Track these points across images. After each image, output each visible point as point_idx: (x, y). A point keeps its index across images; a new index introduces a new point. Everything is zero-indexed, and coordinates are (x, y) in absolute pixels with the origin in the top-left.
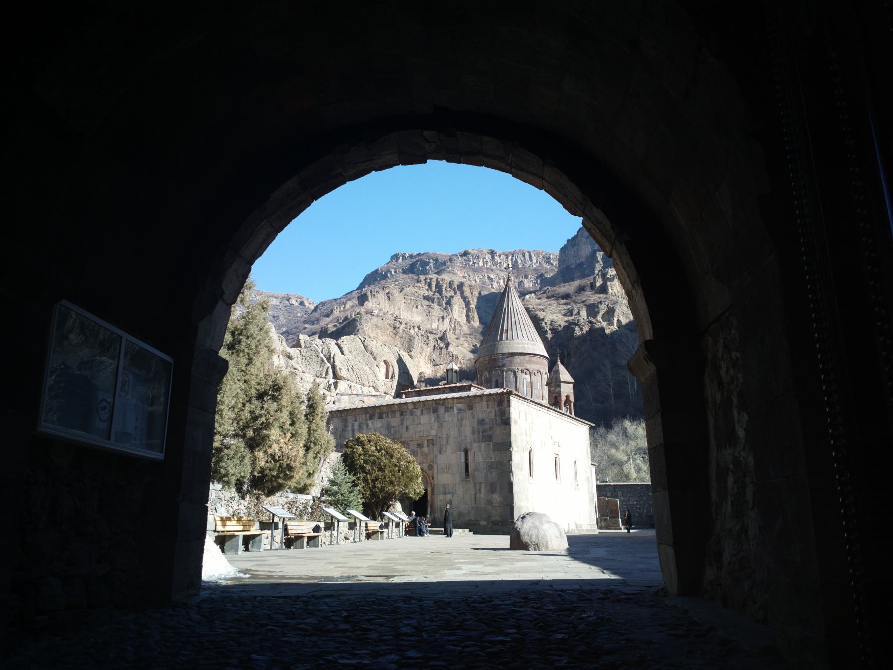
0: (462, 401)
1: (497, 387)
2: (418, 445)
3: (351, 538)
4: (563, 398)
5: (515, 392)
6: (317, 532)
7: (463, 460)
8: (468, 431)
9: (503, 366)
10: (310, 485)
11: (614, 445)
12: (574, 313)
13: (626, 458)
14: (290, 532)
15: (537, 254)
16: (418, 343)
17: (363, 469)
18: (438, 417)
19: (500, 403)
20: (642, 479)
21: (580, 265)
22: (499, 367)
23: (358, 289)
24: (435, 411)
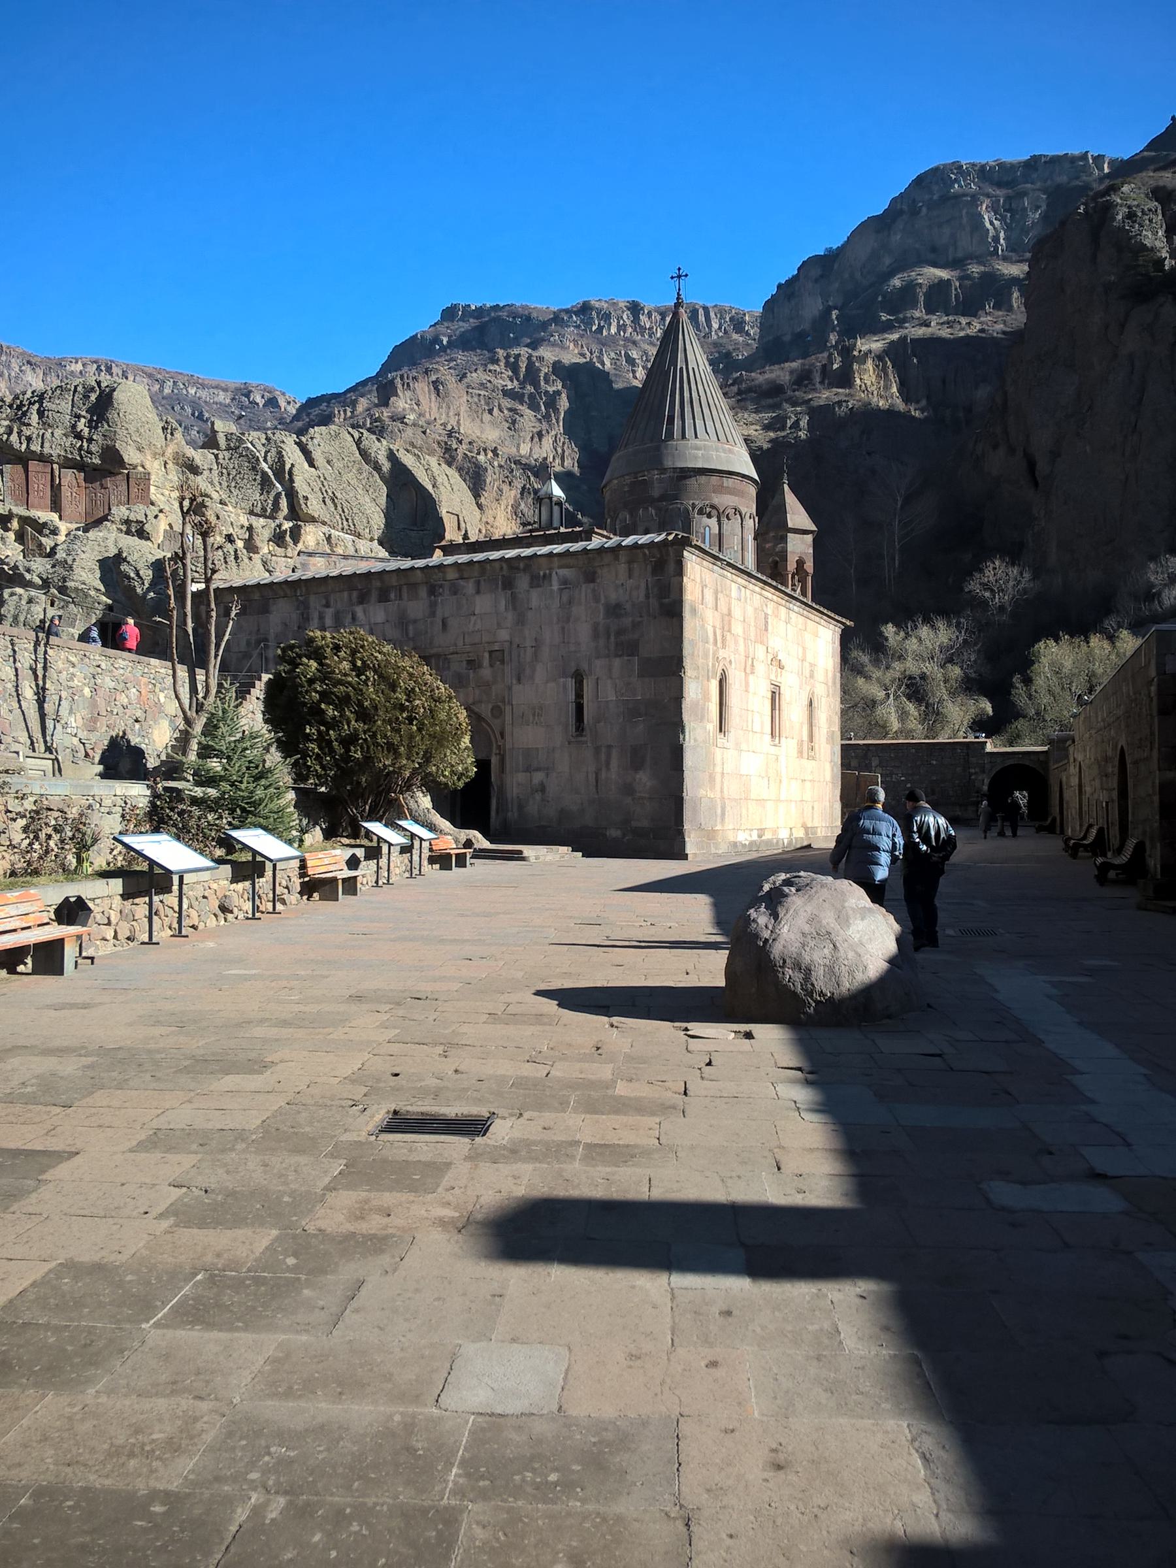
2: (469, 662)
3: (248, 906)
4: (791, 566)
6: (70, 922)
8: (583, 631)
15: (721, 312)
16: (492, 478)
17: (316, 714)
18: (514, 597)
19: (659, 567)
20: (909, 733)
21: (800, 337)
24: (508, 584)
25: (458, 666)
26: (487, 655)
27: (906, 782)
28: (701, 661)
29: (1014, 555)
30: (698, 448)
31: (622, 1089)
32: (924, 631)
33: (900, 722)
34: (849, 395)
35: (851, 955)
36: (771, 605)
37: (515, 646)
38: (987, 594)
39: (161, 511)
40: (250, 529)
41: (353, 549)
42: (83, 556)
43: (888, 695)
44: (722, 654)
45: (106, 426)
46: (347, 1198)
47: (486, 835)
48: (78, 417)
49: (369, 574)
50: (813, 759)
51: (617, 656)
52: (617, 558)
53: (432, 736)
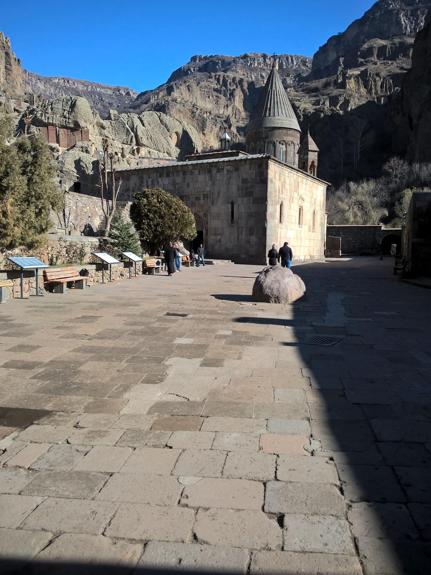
0: (230, 163)
1: (260, 153)
2: (197, 198)
3: (128, 275)
4: (310, 164)
5: (272, 157)
7: (230, 210)
8: (234, 188)
9: (266, 138)
10: (37, 242)
11: (340, 199)
12: (321, 103)
14: (49, 278)
15: (297, 58)
16: (209, 123)
18: (211, 175)
20: (357, 223)
21: (328, 68)
22: (263, 138)
23: (167, 83)
24: (209, 171)
26: (202, 196)
27: (352, 240)
28: (274, 199)
29: (402, 155)
30: (279, 120)
31: (219, 311)
32: (365, 185)
33: (353, 218)
34: (344, 92)
35: (284, 286)
37: (211, 193)
38: (391, 170)
39: (93, 143)
40: (123, 149)
41: (157, 156)
42: (68, 159)
43: (350, 208)
45: (74, 113)
48: (65, 110)
49: (163, 167)
50: (314, 232)
52: (246, 163)
53: (183, 224)
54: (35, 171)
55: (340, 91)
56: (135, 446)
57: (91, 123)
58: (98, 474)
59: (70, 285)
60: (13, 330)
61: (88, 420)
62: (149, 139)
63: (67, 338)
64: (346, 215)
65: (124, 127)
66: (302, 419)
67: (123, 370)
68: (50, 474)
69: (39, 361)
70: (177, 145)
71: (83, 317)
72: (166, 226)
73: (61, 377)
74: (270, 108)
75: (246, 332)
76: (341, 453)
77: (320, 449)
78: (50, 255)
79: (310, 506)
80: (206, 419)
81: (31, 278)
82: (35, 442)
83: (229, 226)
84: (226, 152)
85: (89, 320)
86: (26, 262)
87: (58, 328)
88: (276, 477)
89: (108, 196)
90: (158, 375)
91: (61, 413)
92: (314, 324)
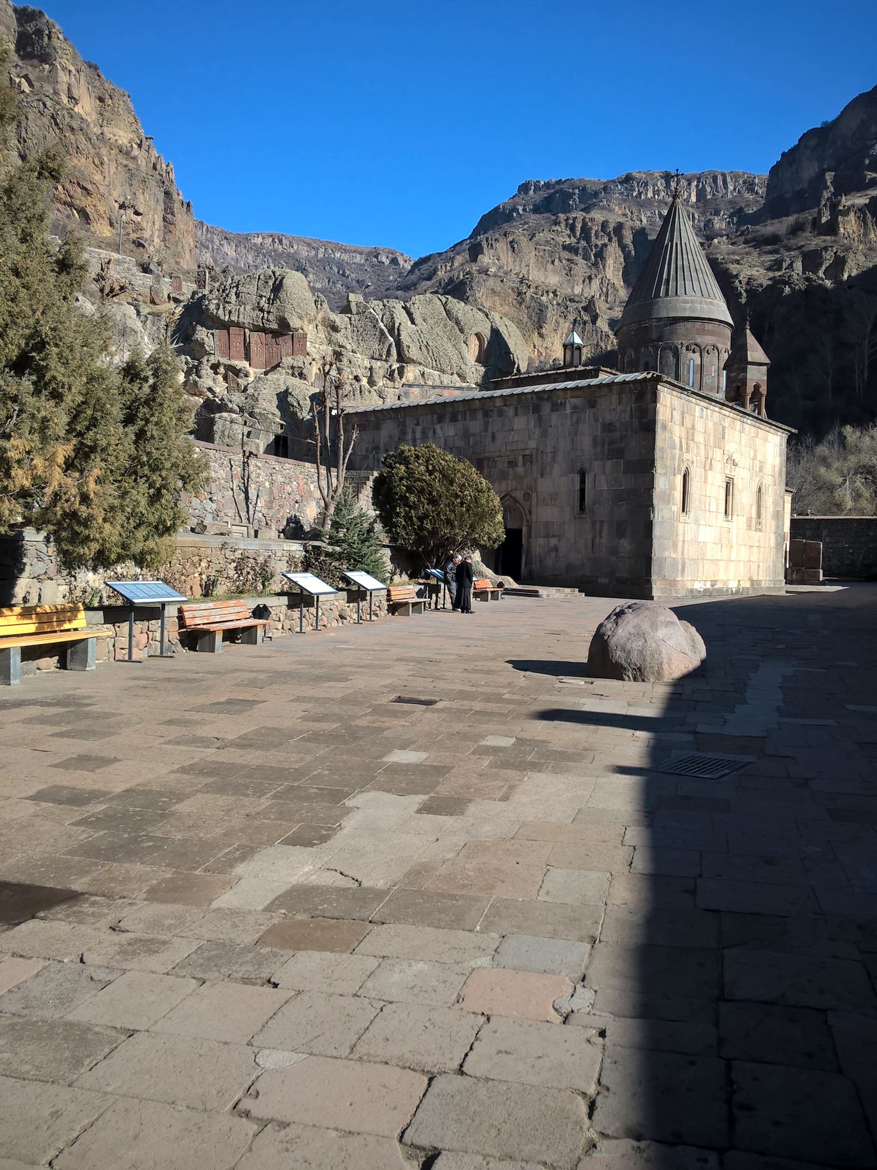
0: (579, 393)
1: (646, 369)
2: (509, 463)
3: (355, 616)
4: (750, 389)
7: (577, 487)
8: (586, 442)
9: (660, 339)
11: (824, 461)
12: (785, 265)
13: (841, 480)
14: (188, 622)
15: (736, 177)
16: (552, 314)
17: (404, 499)
18: (540, 417)
20: (862, 511)
23: (471, 237)
24: (537, 409)
25: (502, 465)
26: (521, 458)
27: (849, 548)
28: (668, 463)
30: (686, 302)
33: (854, 502)
34: (835, 241)
35: (654, 645)
36: (727, 423)
37: (540, 452)
39: (313, 360)
40: (371, 369)
42: (264, 391)
43: (845, 480)
44: (686, 456)
46: (369, 718)
47: (517, 580)
48: (261, 296)
50: (760, 530)
51: (608, 459)
52: (611, 391)
53: (476, 515)
54: (152, 415)
55: (825, 241)
56: (206, 976)
57: (310, 322)
58: (109, 1032)
59: (231, 635)
60: (82, 725)
61: (139, 915)
62: (423, 348)
63: (178, 743)
64: (836, 494)
65: (375, 326)
66: (581, 940)
67: (258, 814)
68: (16, 1024)
69: (104, 789)
70: (478, 360)
71: (230, 702)
72: (441, 520)
73: (131, 826)
74: (668, 280)
75: (544, 742)
76: (636, 1021)
77: (588, 1009)
78: (204, 577)
79: (505, 1137)
80: (376, 928)
81: (153, 622)
82: (21, 956)
83: (575, 518)
84: (573, 369)
85: (236, 708)
86: (143, 589)
87: (171, 722)
88: (461, 1066)
89: (330, 461)
90: (322, 827)
91: (97, 898)
92: (701, 728)
